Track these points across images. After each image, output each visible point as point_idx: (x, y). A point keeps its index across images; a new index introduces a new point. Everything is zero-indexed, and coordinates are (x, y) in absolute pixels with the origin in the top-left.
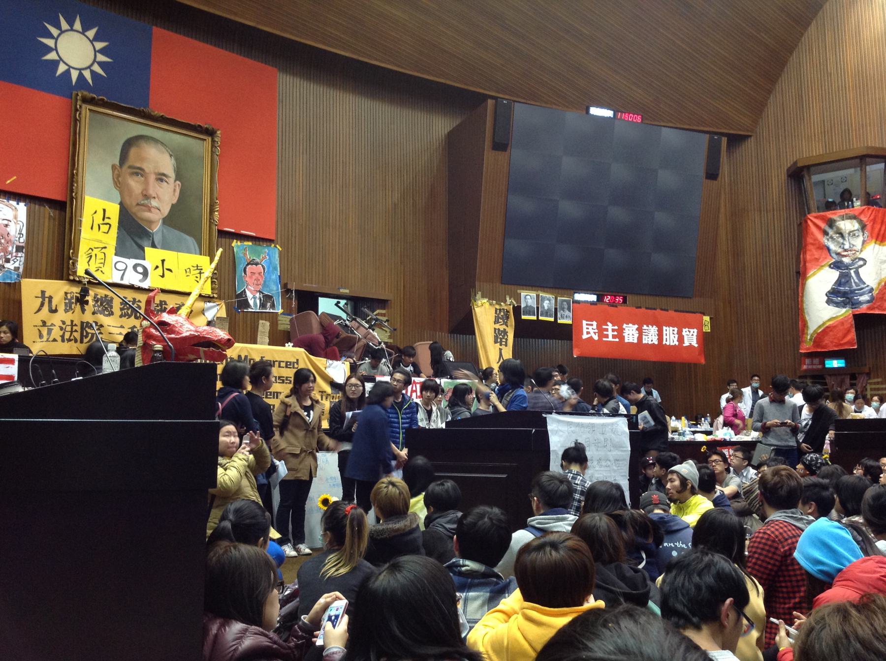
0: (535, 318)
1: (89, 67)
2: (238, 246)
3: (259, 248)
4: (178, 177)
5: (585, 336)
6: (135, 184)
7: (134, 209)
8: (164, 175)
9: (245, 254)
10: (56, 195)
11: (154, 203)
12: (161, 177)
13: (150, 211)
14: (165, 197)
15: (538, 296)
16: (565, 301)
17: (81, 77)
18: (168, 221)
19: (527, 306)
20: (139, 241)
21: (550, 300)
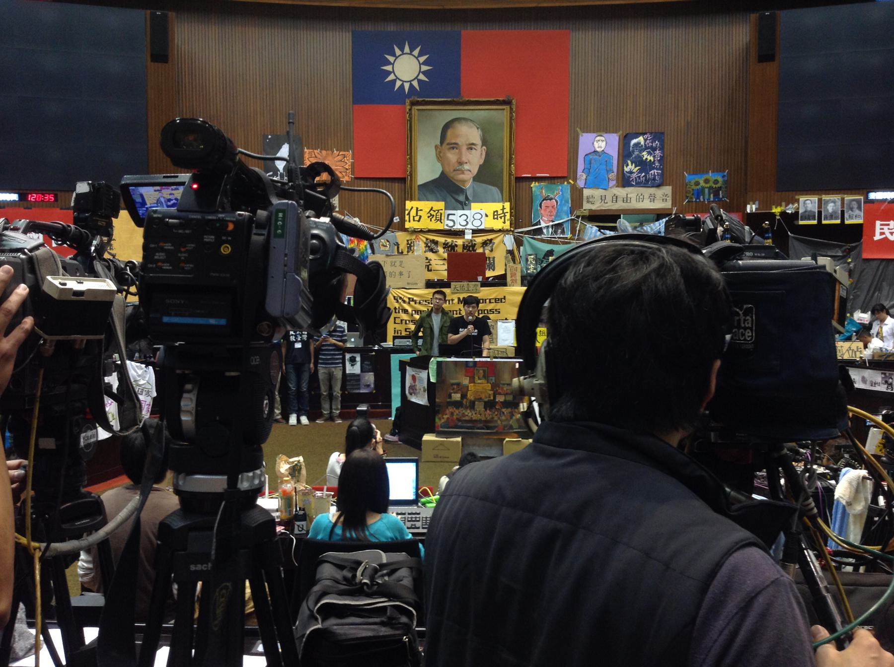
0: (815, 222)
1: (416, 78)
2: (536, 187)
3: (553, 186)
4: (484, 142)
5: (877, 237)
6: (452, 156)
7: (452, 175)
8: (473, 144)
9: (541, 192)
10: (399, 175)
11: (466, 167)
12: (471, 147)
13: (463, 173)
14: (474, 160)
15: (820, 201)
16: (854, 200)
17: (411, 85)
18: (477, 179)
19: (806, 212)
20: (456, 197)
21: (834, 202)
